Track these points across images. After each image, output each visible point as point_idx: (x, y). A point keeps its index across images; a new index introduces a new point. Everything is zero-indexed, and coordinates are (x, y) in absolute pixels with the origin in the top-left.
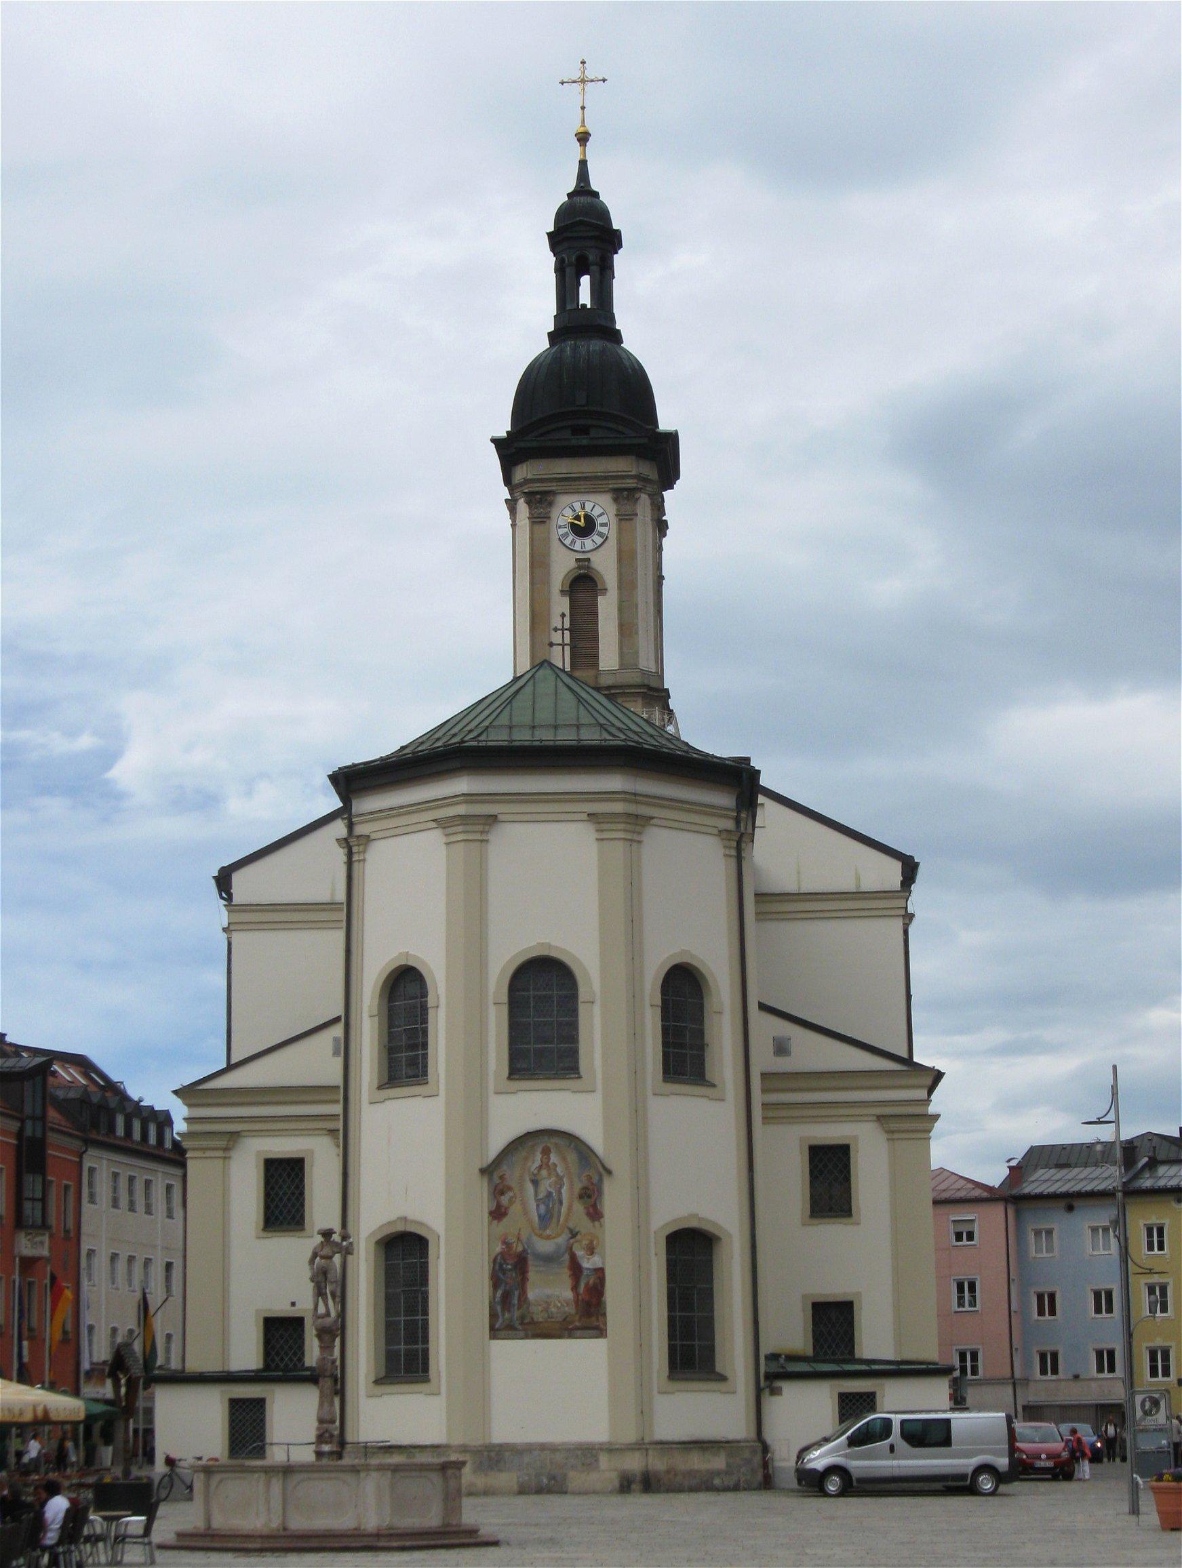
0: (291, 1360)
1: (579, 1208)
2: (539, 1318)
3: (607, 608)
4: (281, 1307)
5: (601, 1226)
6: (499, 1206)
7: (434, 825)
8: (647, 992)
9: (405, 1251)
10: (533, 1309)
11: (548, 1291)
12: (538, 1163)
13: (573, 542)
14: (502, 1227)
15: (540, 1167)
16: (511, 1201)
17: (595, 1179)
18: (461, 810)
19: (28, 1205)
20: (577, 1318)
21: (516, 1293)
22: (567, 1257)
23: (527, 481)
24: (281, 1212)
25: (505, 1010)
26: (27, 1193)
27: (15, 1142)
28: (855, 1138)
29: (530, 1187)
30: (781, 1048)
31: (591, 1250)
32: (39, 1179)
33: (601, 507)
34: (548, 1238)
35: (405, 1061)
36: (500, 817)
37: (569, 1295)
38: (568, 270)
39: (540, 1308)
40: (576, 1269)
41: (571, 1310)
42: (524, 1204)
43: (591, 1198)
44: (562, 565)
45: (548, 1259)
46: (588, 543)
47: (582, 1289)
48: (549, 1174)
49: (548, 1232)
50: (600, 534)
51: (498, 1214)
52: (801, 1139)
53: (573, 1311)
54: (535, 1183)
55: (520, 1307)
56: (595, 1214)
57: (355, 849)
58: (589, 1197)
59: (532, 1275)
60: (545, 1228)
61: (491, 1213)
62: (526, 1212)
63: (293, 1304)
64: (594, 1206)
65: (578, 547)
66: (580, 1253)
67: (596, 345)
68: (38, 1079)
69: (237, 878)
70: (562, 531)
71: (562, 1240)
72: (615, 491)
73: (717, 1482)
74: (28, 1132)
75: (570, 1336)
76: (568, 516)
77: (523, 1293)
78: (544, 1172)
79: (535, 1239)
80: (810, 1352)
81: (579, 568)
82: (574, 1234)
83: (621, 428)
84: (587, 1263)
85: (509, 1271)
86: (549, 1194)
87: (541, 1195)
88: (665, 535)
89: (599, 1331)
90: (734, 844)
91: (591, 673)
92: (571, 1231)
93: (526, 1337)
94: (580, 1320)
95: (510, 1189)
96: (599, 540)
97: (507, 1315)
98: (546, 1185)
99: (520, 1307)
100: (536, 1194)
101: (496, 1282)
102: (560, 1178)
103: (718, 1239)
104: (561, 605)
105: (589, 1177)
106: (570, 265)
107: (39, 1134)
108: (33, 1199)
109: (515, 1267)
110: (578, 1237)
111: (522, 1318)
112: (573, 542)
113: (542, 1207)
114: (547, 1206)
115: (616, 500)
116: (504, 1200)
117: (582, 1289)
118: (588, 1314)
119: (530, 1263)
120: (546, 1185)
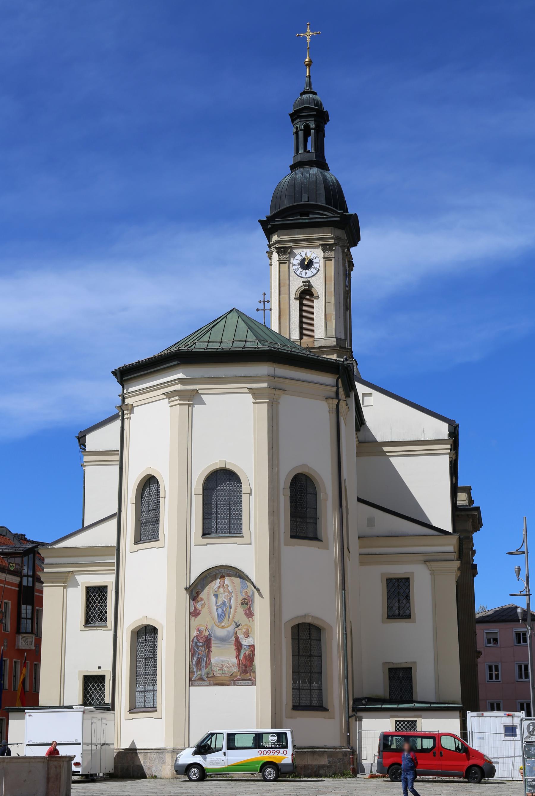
0: (97, 699)
1: (241, 610)
2: (217, 674)
3: (319, 307)
4: (94, 671)
5: (253, 621)
6: (195, 609)
7: (164, 396)
8: (282, 486)
9: (146, 634)
10: (214, 669)
11: (222, 658)
12: (218, 585)
13: (301, 272)
14: (196, 622)
15: (220, 586)
16: (203, 606)
17: (250, 595)
18: (178, 387)
19: (23, 621)
20: (239, 674)
21: (205, 659)
22: (233, 639)
23: (277, 242)
24: (94, 616)
25: (200, 497)
26: (23, 615)
27: (17, 589)
28: (413, 573)
29: (213, 599)
30: (371, 522)
31: (247, 635)
32: (30, 607)
33: (316, 254)
34: (223, 627)
35: (148, 528)
36: (200, 391)
37: (235, 660)
38: (300, 133)
39: (218, 668)
40: (239, 646)
41: (236, 669)
42: (209, 607)
43: (247, 604)
44: (297, 284)
45: (223, 640)
46: (309, 273)
47: (241, 657)
49: (223, 624)
50: (315, 268)
51: (195, 614)
52: (382, 574)
53: (237, 670)
54: (216, 596)
55: (206, 667)
56: (250, 614)
57: (125, 412)
58: (247, 604)
59: (213, 649)
60: (221, 623)
62: (210, 613)
63: (99, 668)
64: (249, 609)
65: (303, 275)
66: (241, 636)
67: (314, 170)
68: (31, 556)
69: (89, 437)
70: (295, 267)
71: (231, 628)
72: (322, 245)
73: (322, 772)
74: (25, 583)
75: (235, 685)
76: (299, 258)
77: (209, 658)
78: (221, 590)
79: (215, 627)
80: (388, 697)
81: (304, 286)
83: (326, 213)
84: (245, 642)
85: (200, 648)
86: (224, 602)
87: (220, 603)
88: (352, 270)
89: (251, 682)
90: (335, 406)
91: (311, 340)
92: (236, 623)
93: (210, 685)
94: (241, 674)
96: (315, 271)
97: (199, 672)
98: (222, 597)
99: (206, 667)
101: (193, 652)
102: (230, 593)
103: (324, 629)
104: (295, 306)
105: (247, 593)
106: (301, 130)
107: (30, 584)
108: (26, 619)
109: (204, 644)
111: (208, 674)
112: (301, 272)
113: (220, 610)
115: (324, 251)
116: (199, 606)
117: (241, 657)
118: (245, 672)
119: (212, 642)
120: (222, 597)
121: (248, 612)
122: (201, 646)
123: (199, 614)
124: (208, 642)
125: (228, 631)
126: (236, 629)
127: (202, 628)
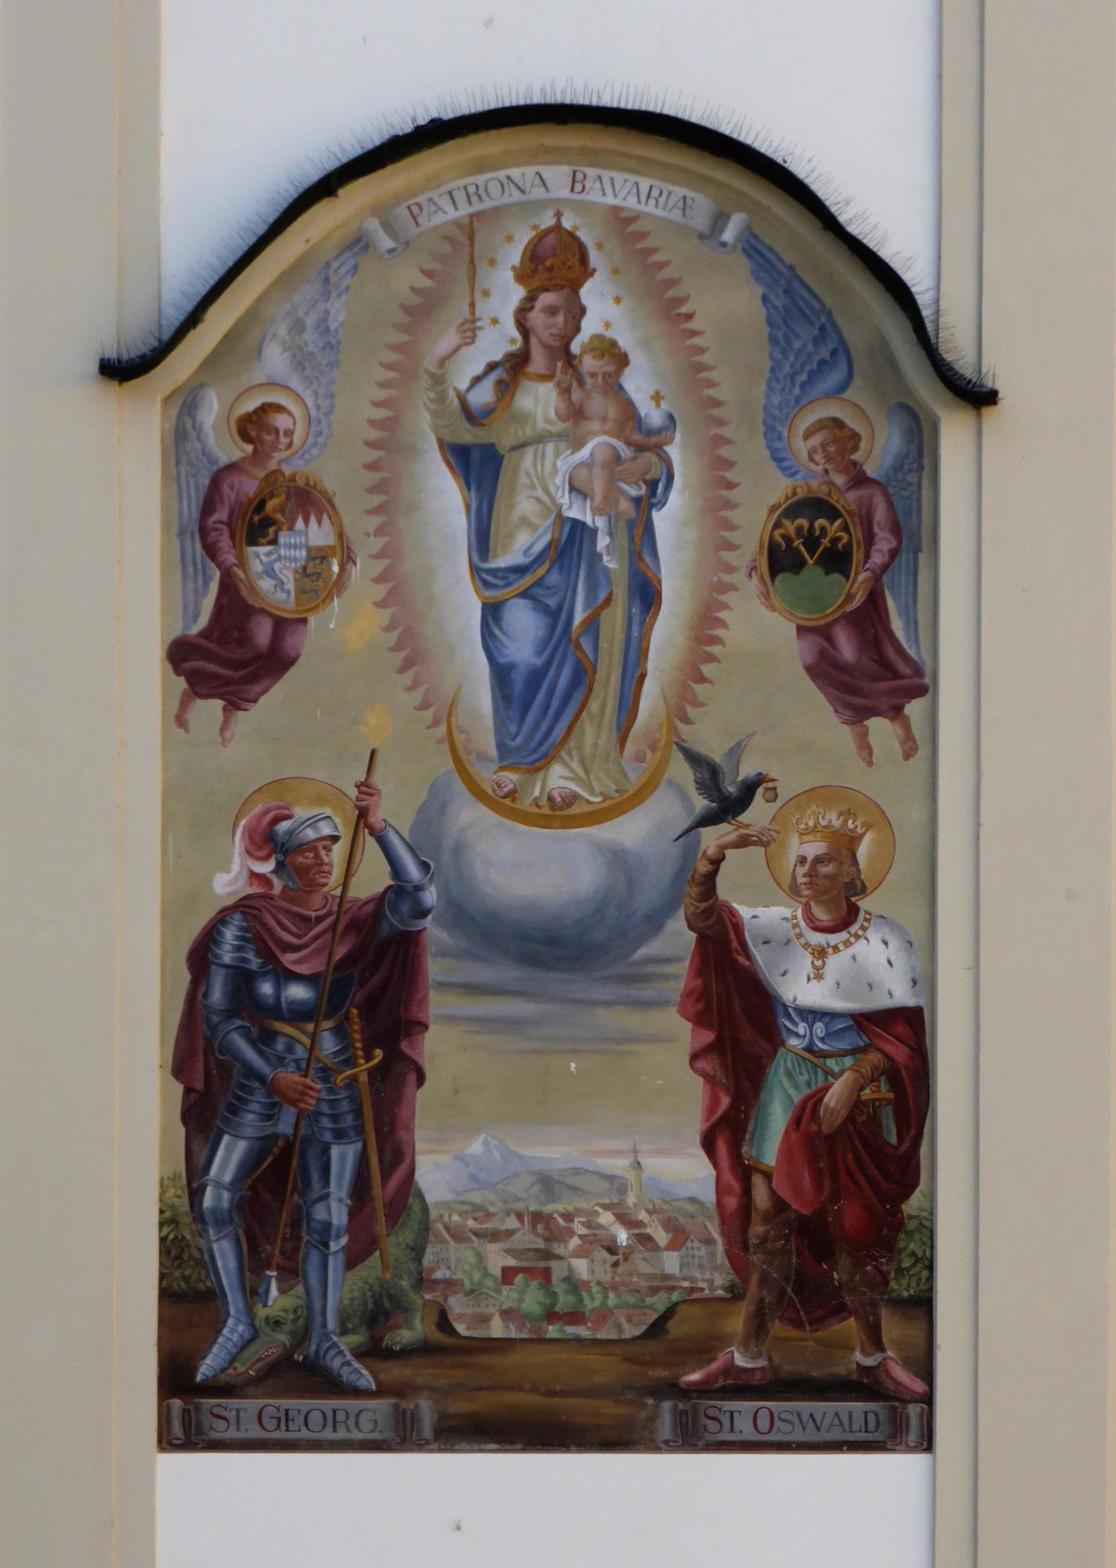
1: (766, 631)
6: (234, 607)
12: (497, 340)
15: (516, 365)
16: (318, 580)
22: (678, 938)
29: (445, 497)
34: (560, 813)
45: (556, 950)
48: (576, 414)
49: (558, 778)
51: (227, 657)
54: (479, 466)
56: (874, 673)
58: (837, 561)
59: (441, 1048)
60: (538, 763)
61: (180, 654)
62: (411, 650)
64: (869, 619)
66: (765, 913)
78: (539, 400)
79: (469, 816)
82: (727, 801)
84: (810, 982)
86: (572, 542)
87: (518, 546)
92: (709, 774)
95: (308, 500)
100: (482, 539)
102: (646, 440)
105: (841, 439)
110: (758, 813)
113: (524, 626)
114: (556, 616)
116: (272, 572)
119: (434, 968)
120: (551, 483)
121: (847, 649)
122: (301, 1014)
123: (275, 662)
124: (376, 972)
125: (617, 858)
126: (711, 838)
127: (317, 820)
